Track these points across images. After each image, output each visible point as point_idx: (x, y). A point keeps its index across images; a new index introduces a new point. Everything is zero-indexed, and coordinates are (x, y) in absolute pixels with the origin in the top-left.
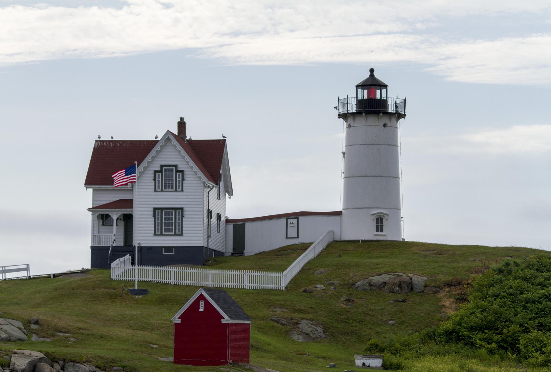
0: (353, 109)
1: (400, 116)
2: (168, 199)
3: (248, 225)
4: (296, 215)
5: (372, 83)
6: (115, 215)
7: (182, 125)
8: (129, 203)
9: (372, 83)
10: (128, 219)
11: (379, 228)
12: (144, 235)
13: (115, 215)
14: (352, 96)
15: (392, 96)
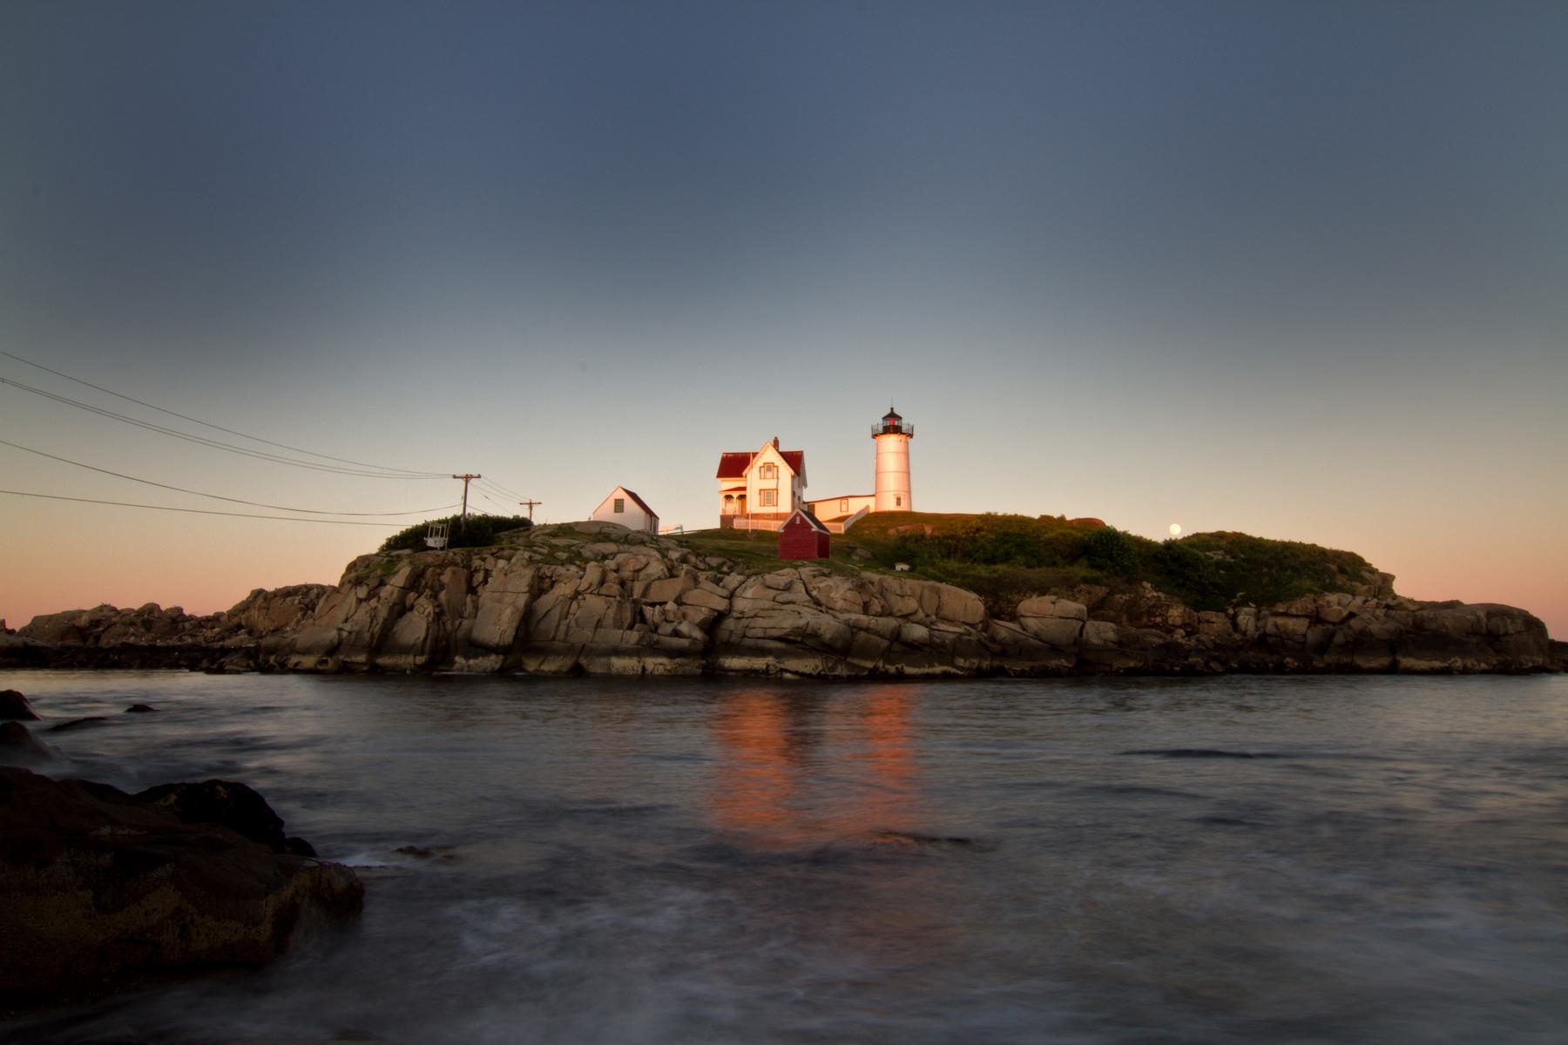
0: (881, 429)
1: (911, 436)
2: (771, 484)
3: (817, 506)
4: (846, 498)
5: (892, 415)
6: (735, 495)
7: (776, 444)
8: (744, 489)
9: (892, 415)
10: (742, 497)
11: (898, 503)
12: (753, 505)
13: (735, 495)
14: (879, 423)
15: (905, 424)
